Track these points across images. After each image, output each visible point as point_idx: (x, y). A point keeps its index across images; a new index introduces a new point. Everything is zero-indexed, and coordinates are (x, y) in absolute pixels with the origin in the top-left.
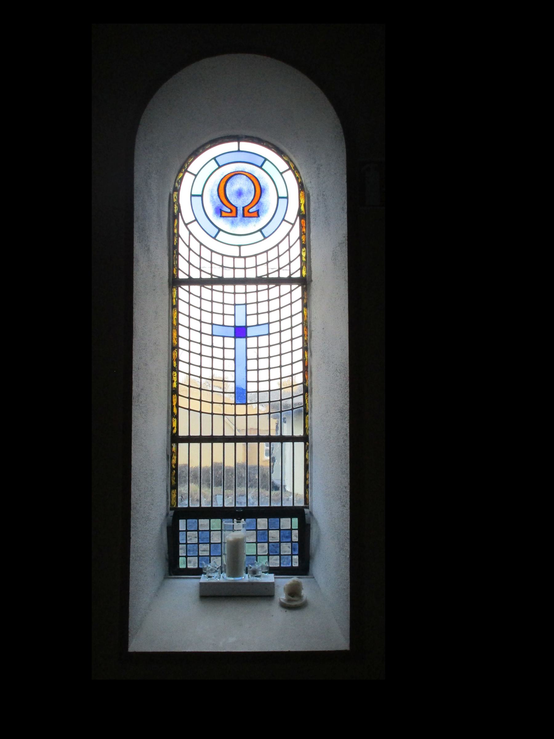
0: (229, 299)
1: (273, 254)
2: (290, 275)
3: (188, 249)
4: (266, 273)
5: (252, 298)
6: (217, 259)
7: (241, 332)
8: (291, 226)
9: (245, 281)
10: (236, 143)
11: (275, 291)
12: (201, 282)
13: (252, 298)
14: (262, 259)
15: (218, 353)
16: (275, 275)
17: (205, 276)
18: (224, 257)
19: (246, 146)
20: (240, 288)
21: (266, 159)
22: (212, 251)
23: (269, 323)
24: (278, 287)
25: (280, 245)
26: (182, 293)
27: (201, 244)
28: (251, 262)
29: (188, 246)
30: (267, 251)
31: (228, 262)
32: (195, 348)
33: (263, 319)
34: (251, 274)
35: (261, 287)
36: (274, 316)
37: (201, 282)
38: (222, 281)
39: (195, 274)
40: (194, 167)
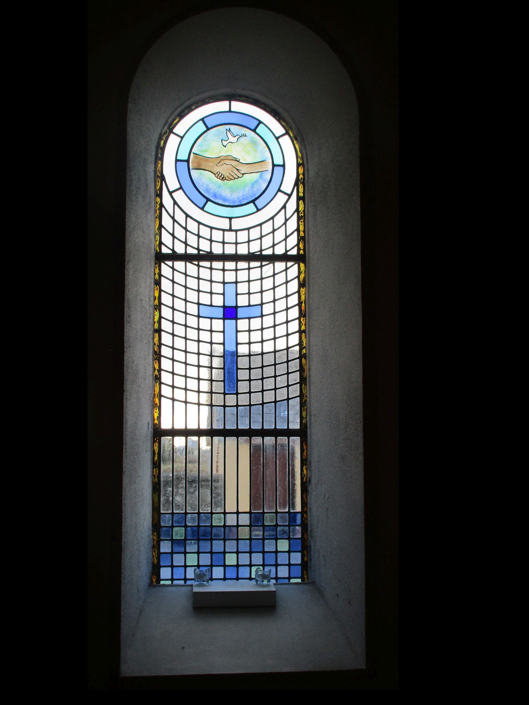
6: (205, 232)
9: (236, 258)
14: (255, 233)
16: (269, 252)
17: (190, 251)
31: (217, 235)
38: (210, 257)
39: (180, 249)
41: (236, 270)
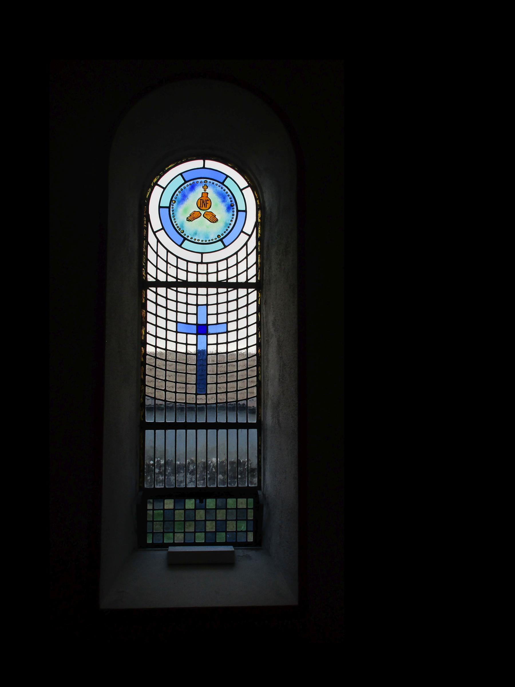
0: (192, 299)
1: (232, 261)
2: (247, 280)
5: (212, 300)
6: (182, 264)
9: (207, 285)
10: (202, 161)
11: (233, 295)
12: (167, 285)
13: (212, 300)
14: (222, 265)
16: (234, 280)
17: (170, 279)
19: (210, 164)
20: (202, 291)
22: (178, 257)
23: (227, 322)
26: (151, 295)
27: (168, 251)
28: (212, 268)
29: (157, 253)
31: (192, 267)
33: (222, 318)
34: (212, 278)
35: (221, 290)
36: (232, 316)
37: (167, 285)
38: (186, 284)
39: (162, 278)
40: (164, 181)
41: (207, 295)
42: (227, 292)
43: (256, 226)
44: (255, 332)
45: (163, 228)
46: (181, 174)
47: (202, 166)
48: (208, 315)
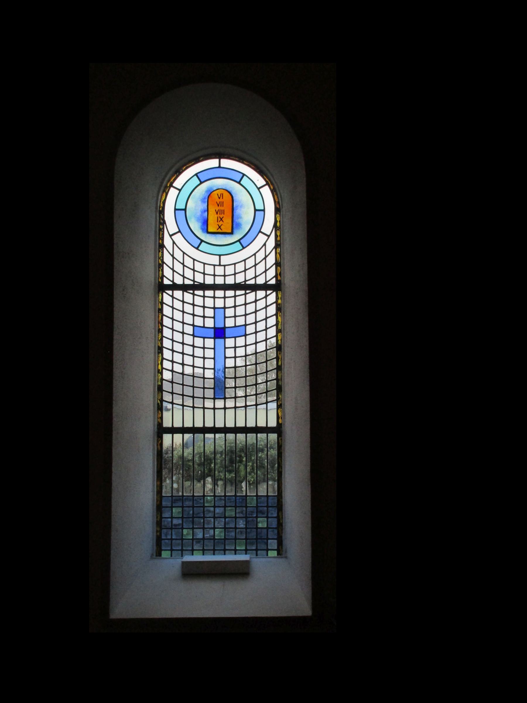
0: (209, 302)
3: (171, 258)
4: (244, 280)
6: (199, 267)
7: (220, 333)
8: (267, 237)
9: (225, 287)
10: (217, 160)
11: (251, 297)
12: (184, 288)
13: (230, 302)
14: (240, 267)
15: (199, 352)
16: (252, 282)
17: (187, 282)
18: (206, 265)
19: (226, 163)
20: (220, 293)
21: (244, 175)
22: (194, 260)
23: (246, 325)
24: (254, 293)
25: (257, 254)
26: (167, 299)
27: (184, 253)
29: (173, 256)
30: (245, 260)
31: (209, 270)
32: (178, 347)
34: (230, 281)
35: (238, 292)
36: (251, 319)
37: (184, 288)
38: (203, 287)
39: (179, 280)
40: (179, 183)
41: (225, 298)
42: (245, 294)
43: (275, 226)
44: (275, 334)
45: (180, 231)
46: (196, 175)
47: (218, 166)
48: (225, 317)
